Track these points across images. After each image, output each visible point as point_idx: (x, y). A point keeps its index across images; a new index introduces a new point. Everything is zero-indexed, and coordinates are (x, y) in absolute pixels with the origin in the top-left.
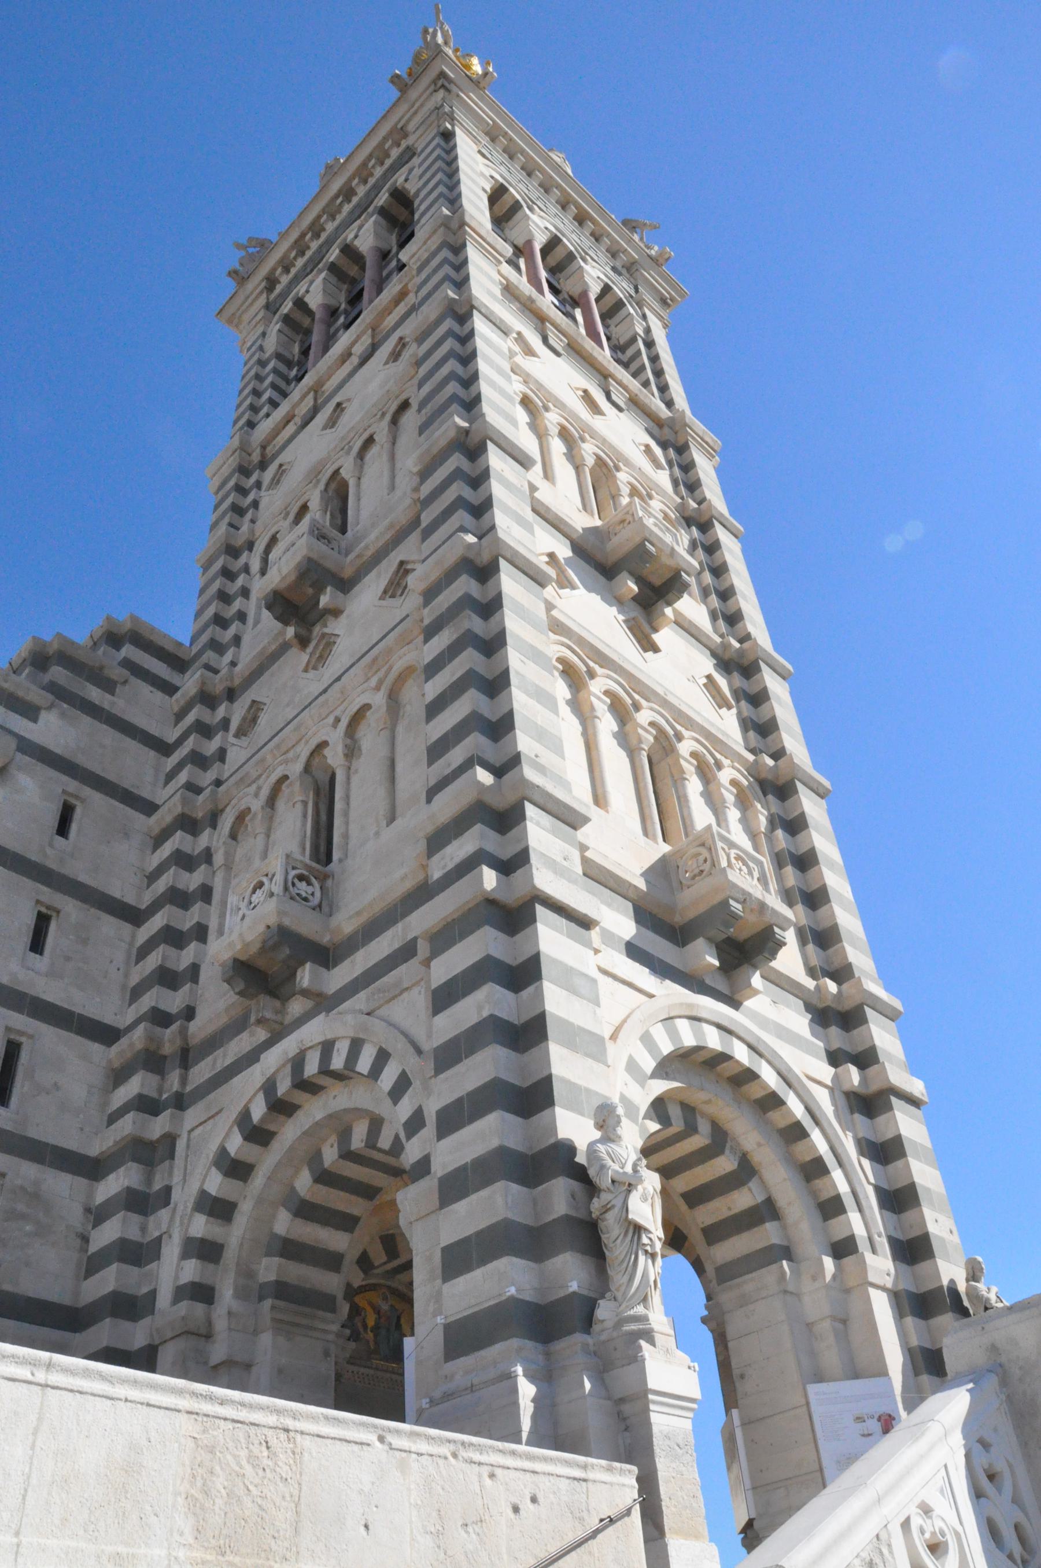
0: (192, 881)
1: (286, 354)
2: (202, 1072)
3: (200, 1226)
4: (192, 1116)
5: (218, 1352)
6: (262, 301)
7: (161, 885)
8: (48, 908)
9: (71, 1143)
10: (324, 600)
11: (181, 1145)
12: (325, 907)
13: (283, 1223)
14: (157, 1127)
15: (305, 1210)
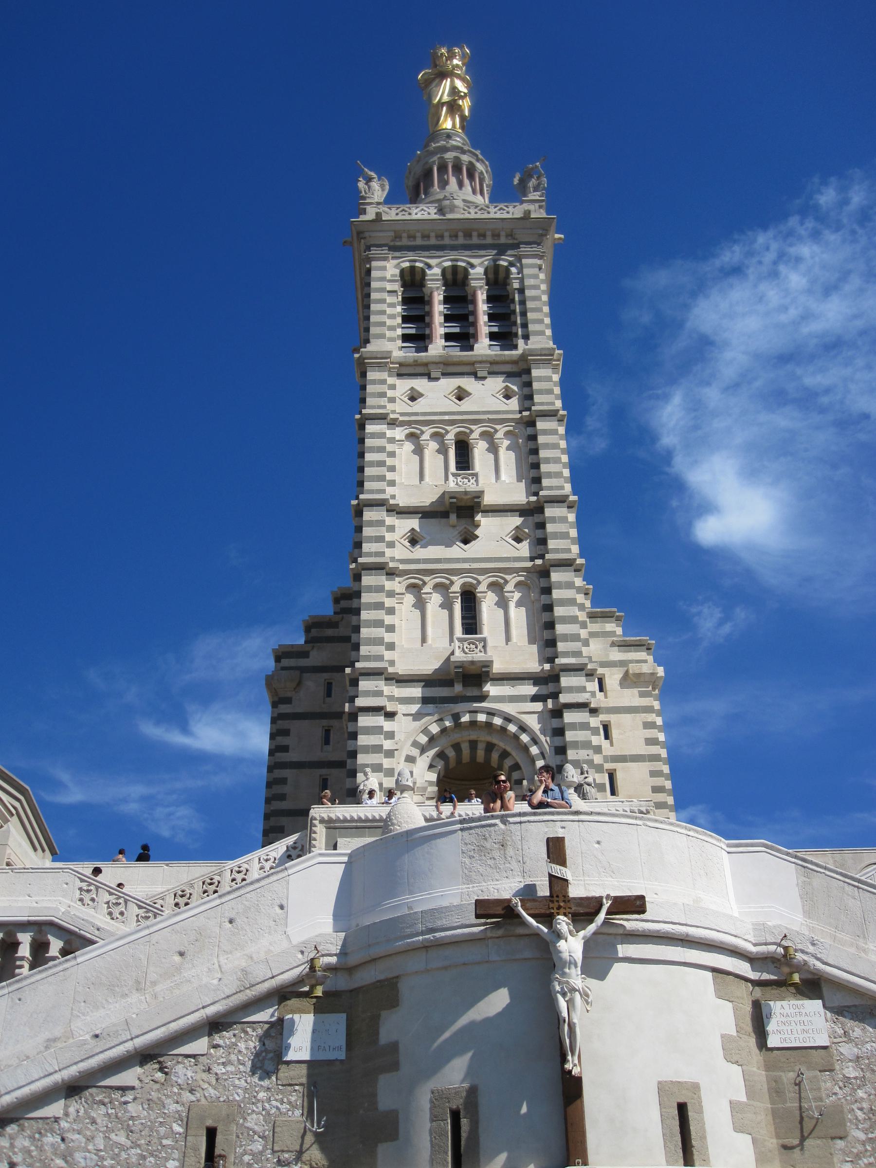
8: (329, 727)
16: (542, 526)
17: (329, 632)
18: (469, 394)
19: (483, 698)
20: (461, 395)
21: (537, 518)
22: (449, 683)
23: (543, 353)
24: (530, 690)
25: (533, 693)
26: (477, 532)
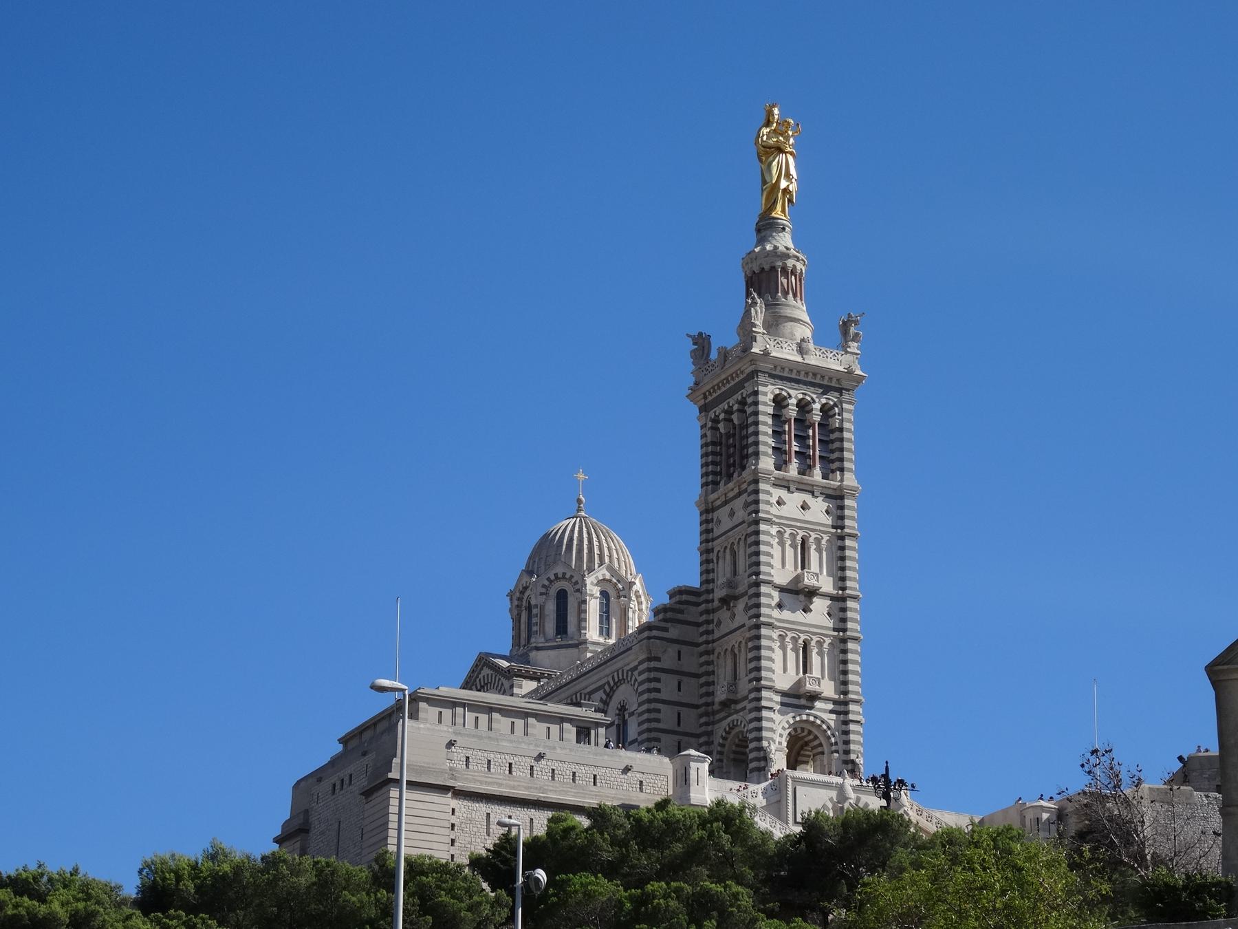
0: (710, 668)
1: (715, 440)
2: (717, 717)
3: (719, 748)
4: (716, 726)
5: (725, 770)
6: (702, 402)
7: (703, 669)
9: (694, 732)
10: (732, 605)
11: (714, 733)
12: (735, 692)
13: (734, 748)
14: (710, 728)
15: (735, 752)
16: (844, 610)
17: (679, 616)
18: (809, 508)
19: (811, 708)
20: (804, 507)
21: (841, 604)
22: (798, 697)
23: (853, 489)
24: (830, 706)
25: (830, 708)
26: (811, 607)
